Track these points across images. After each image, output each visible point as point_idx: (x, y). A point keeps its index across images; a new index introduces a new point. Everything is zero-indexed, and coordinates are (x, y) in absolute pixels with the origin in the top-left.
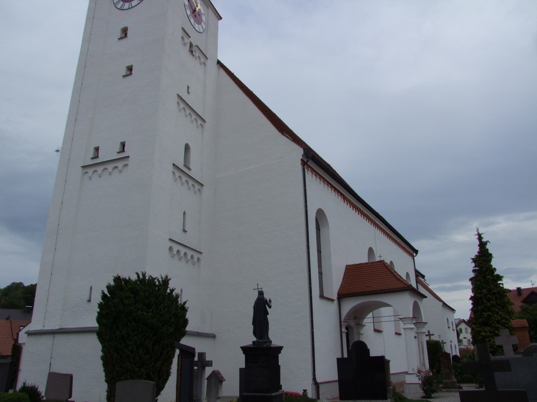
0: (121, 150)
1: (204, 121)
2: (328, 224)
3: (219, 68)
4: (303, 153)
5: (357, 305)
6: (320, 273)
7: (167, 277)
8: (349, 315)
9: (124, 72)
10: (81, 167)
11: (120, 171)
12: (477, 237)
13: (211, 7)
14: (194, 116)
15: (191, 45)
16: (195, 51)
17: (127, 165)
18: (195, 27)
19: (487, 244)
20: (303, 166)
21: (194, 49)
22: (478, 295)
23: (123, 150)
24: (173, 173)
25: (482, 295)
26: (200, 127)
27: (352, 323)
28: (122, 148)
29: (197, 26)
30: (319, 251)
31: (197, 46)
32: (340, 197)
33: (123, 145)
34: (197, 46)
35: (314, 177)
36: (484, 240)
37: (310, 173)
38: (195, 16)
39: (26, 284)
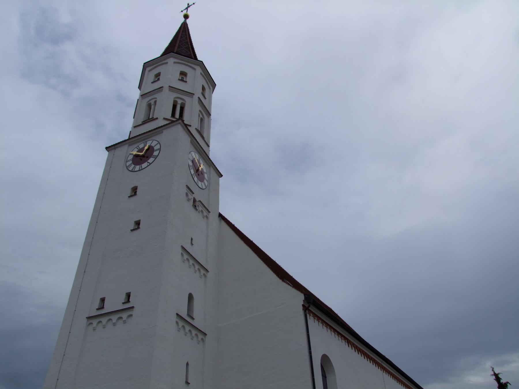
0: (126, 301)
1: (207, 271)
2: (334, 370)
3: (220, 220)
9: (132, 226)
10: (87, 318)
11: (125, 322)
13: (212, 167)
14: (197, 267)
15: (195, 201)
16: (198, 206)
17: (131, 315)
18: (198, 184)
21: (197, 204)
23: (128, 301)
24: (177, 322)
26: (203, 277)
28: (127, 299)
29: (200, 184)
31: (200, 201)
32: (344, 341)
33: (128, 295)
34: (200, 201)
35: (316, 322)
37: (312, 318)
38: (198, 175)
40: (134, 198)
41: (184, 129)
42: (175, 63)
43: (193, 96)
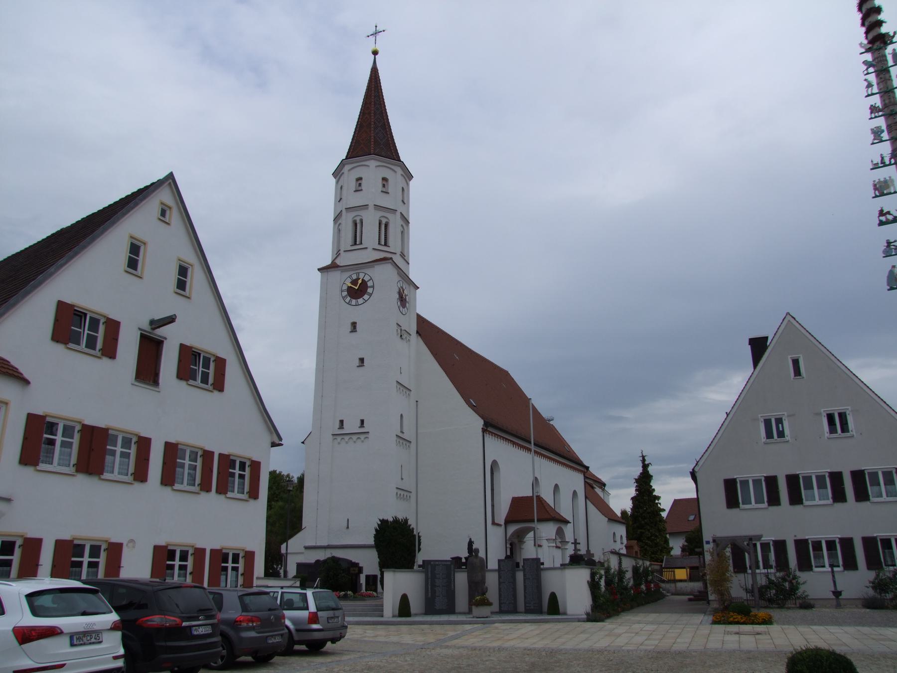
2: (499, 469)
4: (483, 424)
5: (520, 528)
6: (493, 506)
7: (406, 518)
8: (512, 535)
9: (357, 363)
11: (363, 441)
12: (641, 459)
19: (649, 466)
20: (483, 433)
21: (403, 332)
22: (636, 514)
25: (639, 514)
27: (516, 541)
29: (401, 308)
30: (492, 490)
31: (405, 330)
33: (362, 422)
36: (646, 462)
37: (488, 435)
39: (375, 533)
40: (354, 334)
41: (394, 266)
42: (377, 166)
43: (395, 213)
